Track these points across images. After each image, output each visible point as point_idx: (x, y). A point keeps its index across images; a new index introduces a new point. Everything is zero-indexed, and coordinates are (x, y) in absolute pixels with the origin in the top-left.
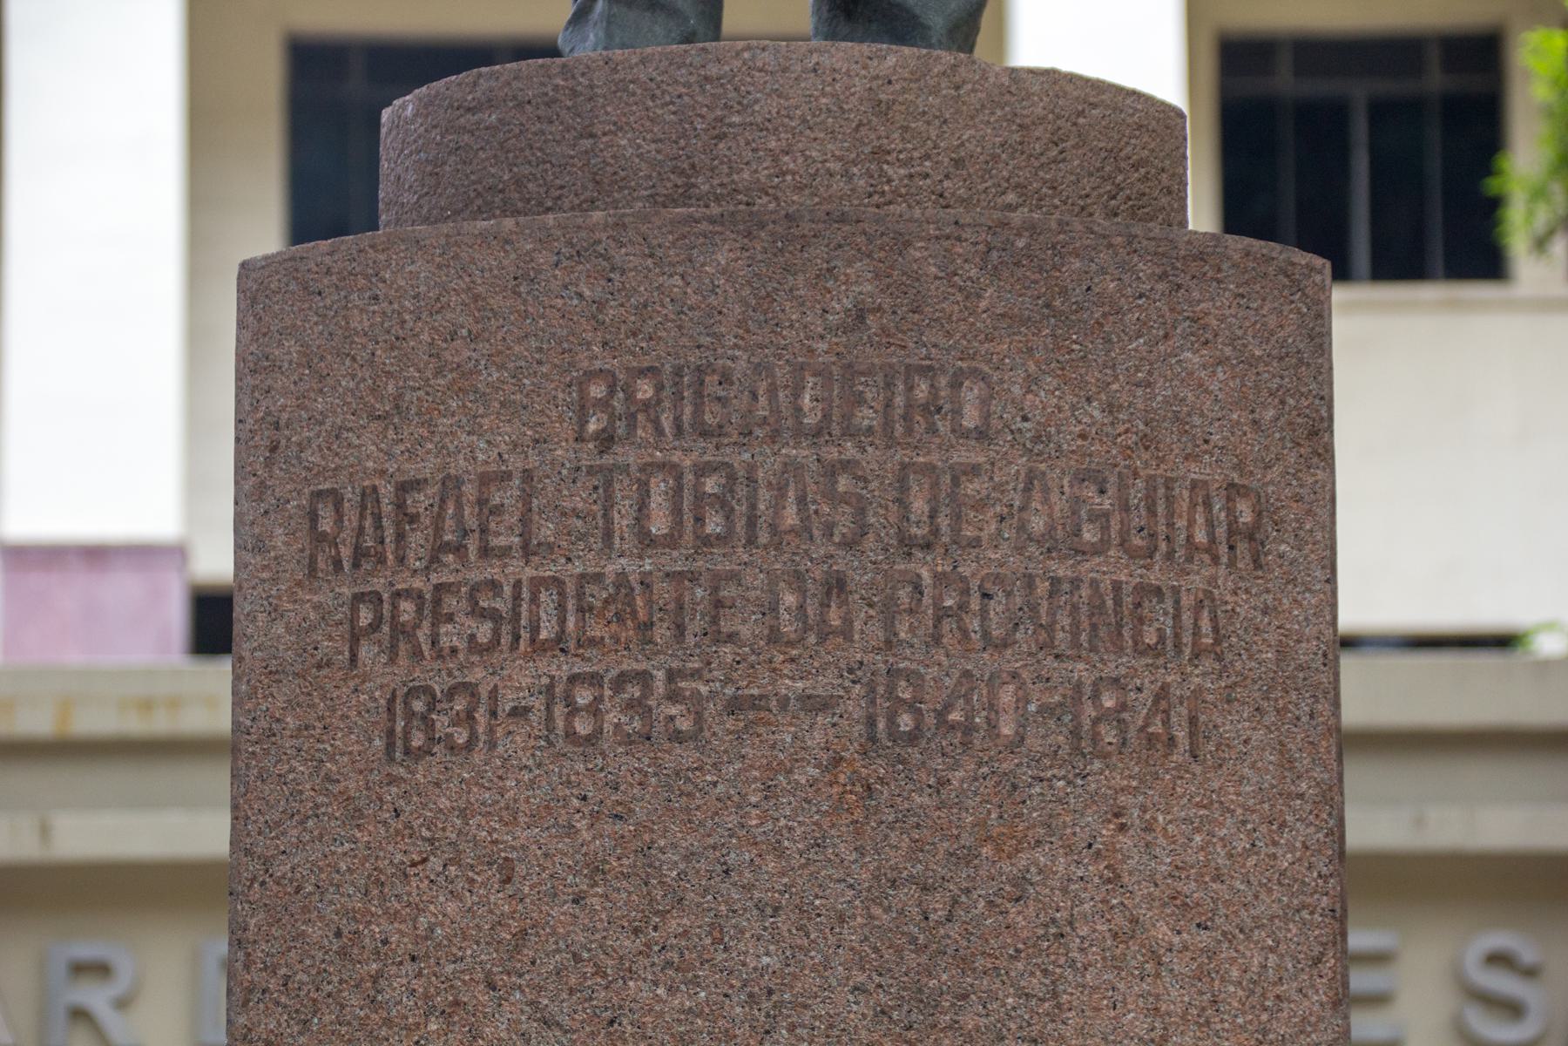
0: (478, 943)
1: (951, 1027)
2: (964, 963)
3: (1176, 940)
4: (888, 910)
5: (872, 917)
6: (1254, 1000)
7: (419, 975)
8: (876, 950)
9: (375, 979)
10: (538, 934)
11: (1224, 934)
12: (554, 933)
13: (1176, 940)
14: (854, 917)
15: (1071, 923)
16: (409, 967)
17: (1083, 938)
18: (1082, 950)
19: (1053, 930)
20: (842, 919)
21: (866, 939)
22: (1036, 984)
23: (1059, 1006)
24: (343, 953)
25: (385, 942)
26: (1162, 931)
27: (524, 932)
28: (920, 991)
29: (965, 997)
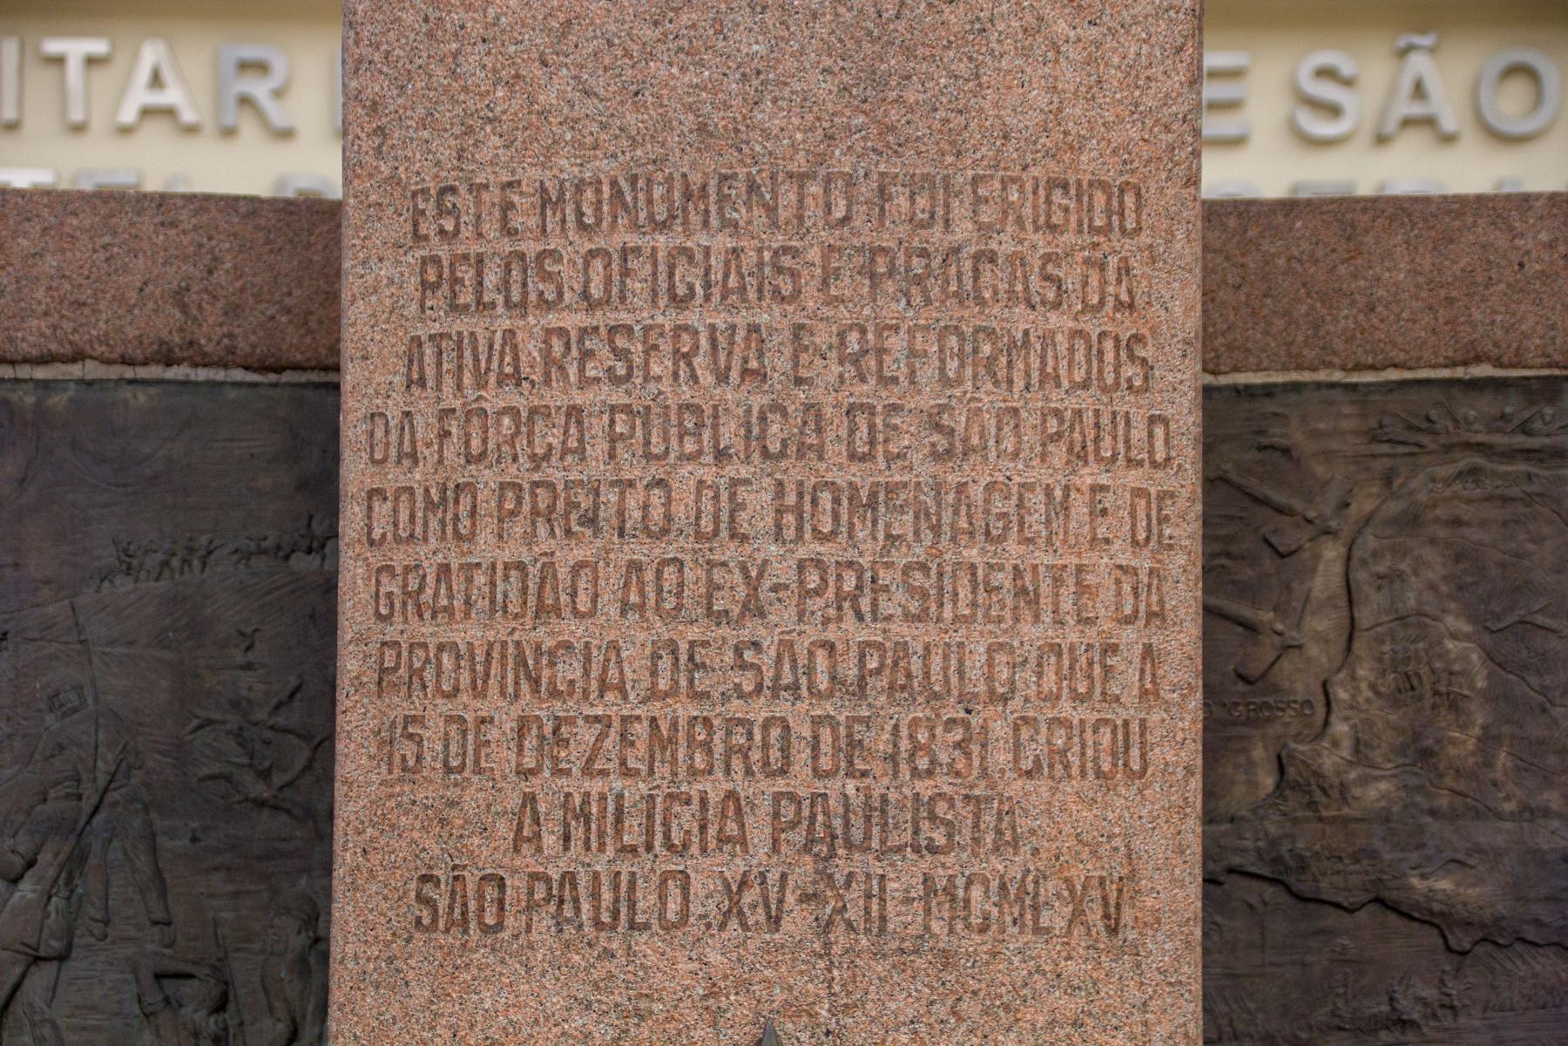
0: (534, 30)
1: (897, 101)
2: (908, 51)
3: (1072, 34)
4: (850, 9)
5: (837, 15)
6: (1130, 80)
7: (489, 53)
8: (841, 41)
9: (455, 55)
10: (579, 24)
11: (1109, 29)
12: (592, 23)
13: (1072, 34)
14: (824, 14)
15: (991, 21)
16: (481, 47)
17: (1000, 33)
18: (999, 42)
19: (977, 26)
20: (814, 16)
21: (833, 32)
22: (963, 68)
23: (980, 85)
24: (430, 35)
25: (462, 27)
26: (1061, 27)
27: (569, 22)
28: (874, 73)
29: (908, 78)
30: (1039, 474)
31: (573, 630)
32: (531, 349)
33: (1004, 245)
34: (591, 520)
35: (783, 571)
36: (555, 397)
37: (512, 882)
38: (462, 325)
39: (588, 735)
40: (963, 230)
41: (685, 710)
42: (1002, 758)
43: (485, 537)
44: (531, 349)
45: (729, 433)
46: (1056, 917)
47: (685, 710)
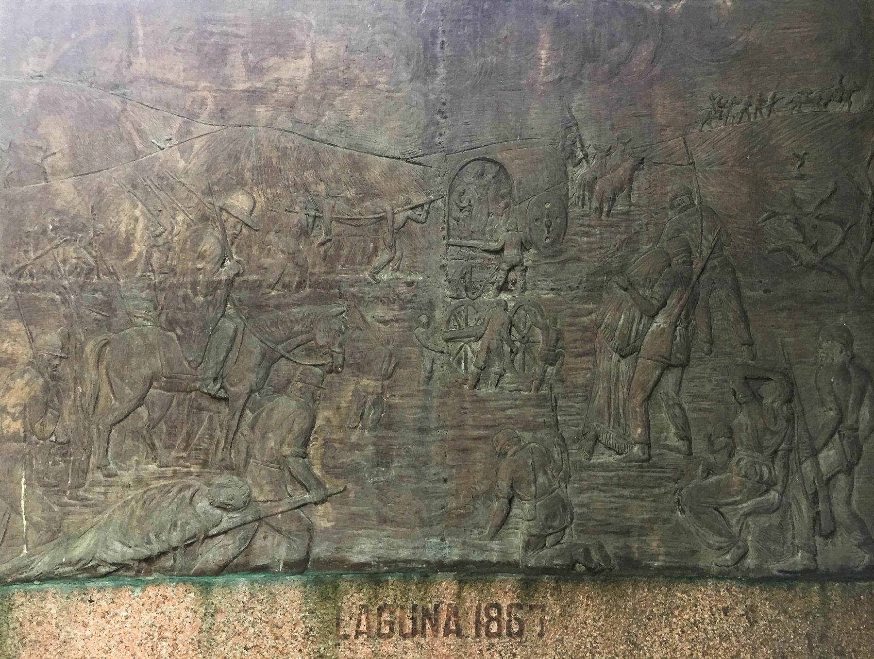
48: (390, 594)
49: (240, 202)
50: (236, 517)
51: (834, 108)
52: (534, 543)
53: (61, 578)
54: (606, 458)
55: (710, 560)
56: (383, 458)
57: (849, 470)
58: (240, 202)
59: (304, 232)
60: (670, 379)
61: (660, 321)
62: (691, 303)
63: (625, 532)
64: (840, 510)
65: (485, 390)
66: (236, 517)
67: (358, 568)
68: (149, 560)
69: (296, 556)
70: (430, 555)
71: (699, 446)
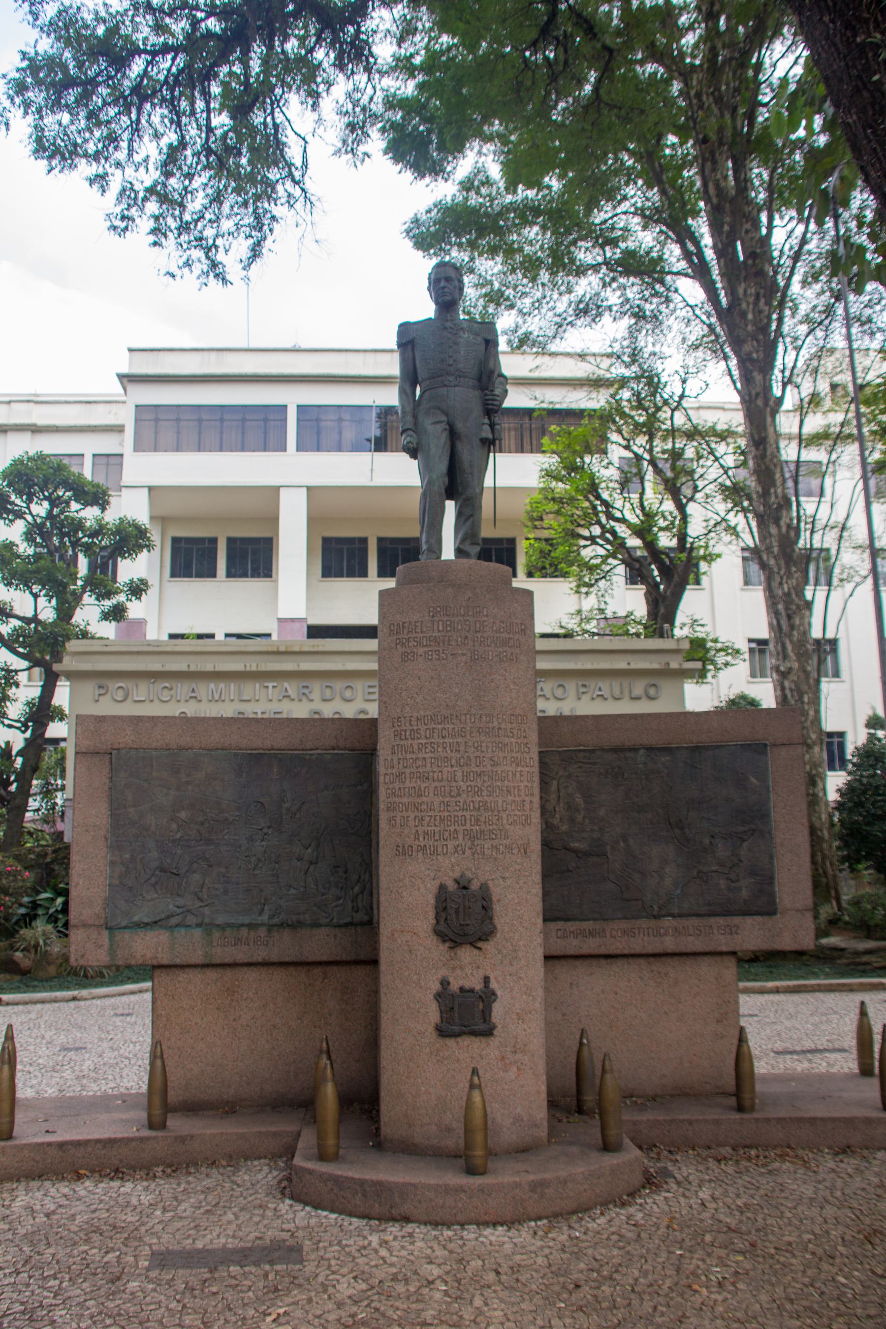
30: (511, 768)
31: (425, 799)
32: (416, 747)
33: (503, 726)
34: (428, 778)
35: (464, 788)
36: (420, 756)
37: (415, 847)
38: (402, 743)
39: (428, 819)
40: (496, 723)
41: (446, 814)
42: (505, 822)
43: (407, 782)
44: (416, 747)
45: (453, 762)
46: (515, 851)
47: (446, 814)
48: (228, 931)
49: (183, 815)
50: (181, 910)
51: (359, 787)
52: (271, 917)
53: (129, 928)
54: (293, 891)
55: (323, 921)
56: (226, 892)
57: (362, 893)
58: (183, 815)
59: (202, 824)
60: (312, 867)
61: (309, 850)
62: (318, 846)
63: (299, 914)
64: (360, 904)
65: (256, 872)
66: (181, 910)
67: (218, 926)
68: (156, 922)
69: (199, 921)
70: (240, 922)
71: (320, 887)
